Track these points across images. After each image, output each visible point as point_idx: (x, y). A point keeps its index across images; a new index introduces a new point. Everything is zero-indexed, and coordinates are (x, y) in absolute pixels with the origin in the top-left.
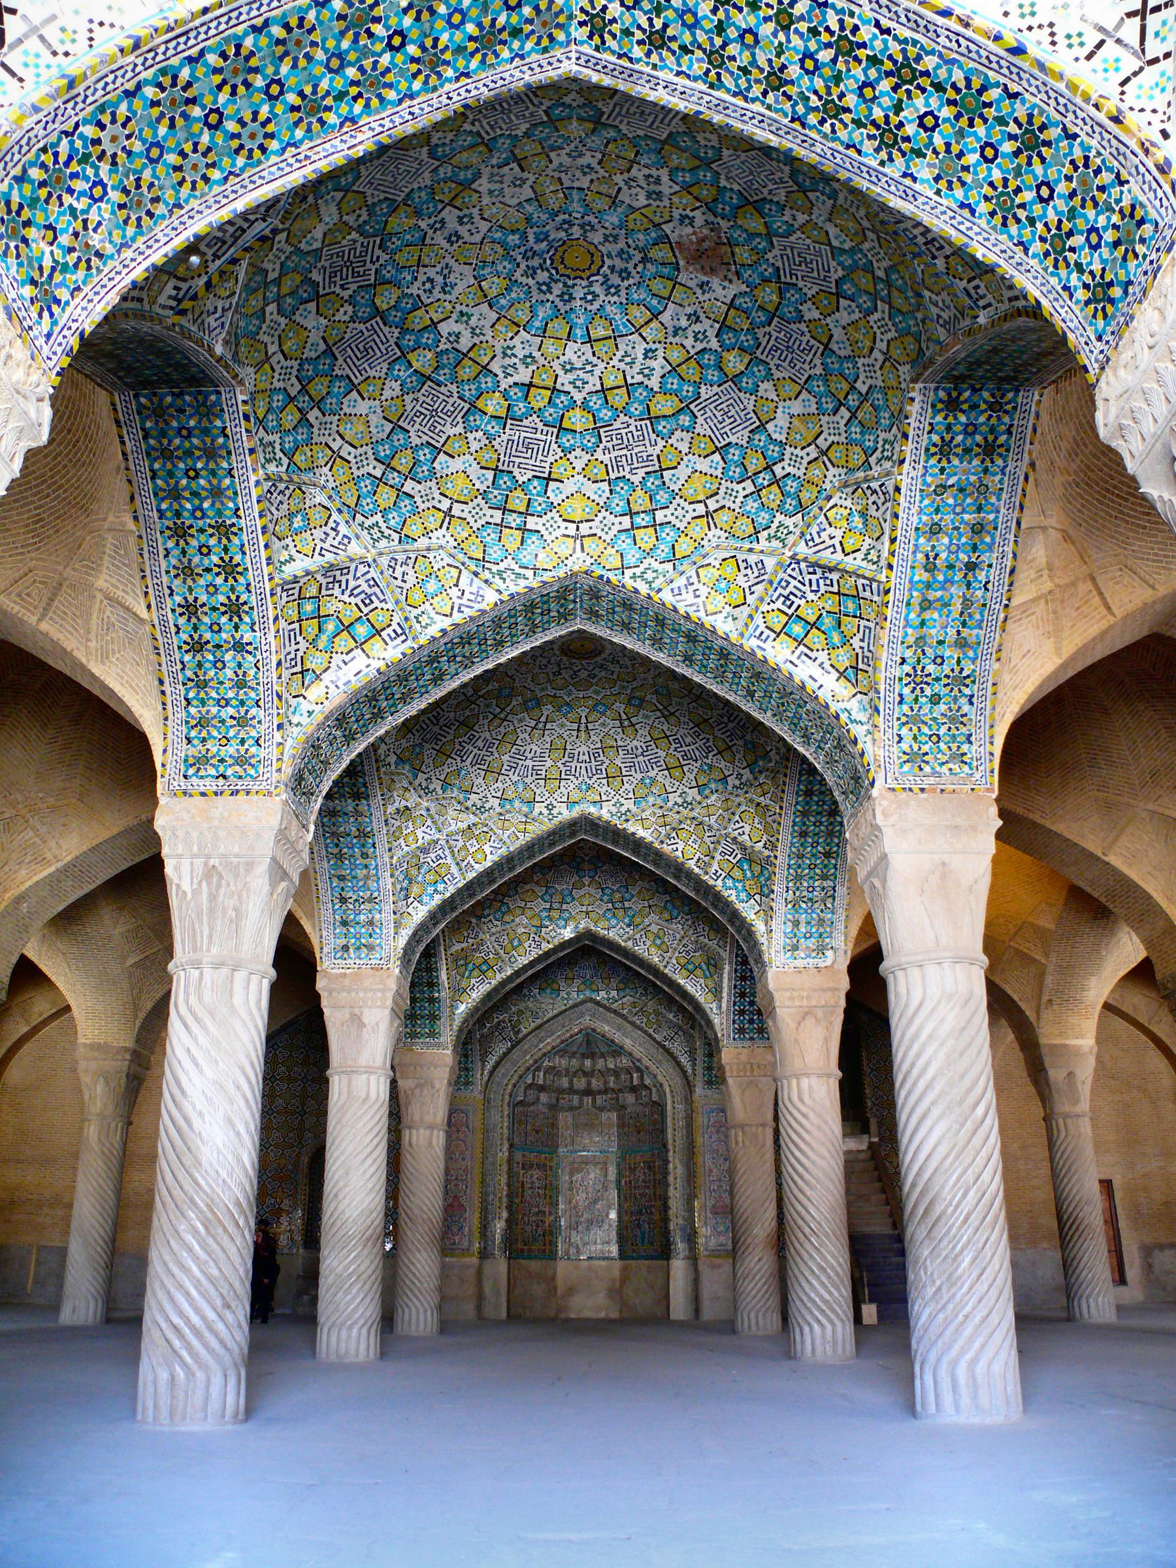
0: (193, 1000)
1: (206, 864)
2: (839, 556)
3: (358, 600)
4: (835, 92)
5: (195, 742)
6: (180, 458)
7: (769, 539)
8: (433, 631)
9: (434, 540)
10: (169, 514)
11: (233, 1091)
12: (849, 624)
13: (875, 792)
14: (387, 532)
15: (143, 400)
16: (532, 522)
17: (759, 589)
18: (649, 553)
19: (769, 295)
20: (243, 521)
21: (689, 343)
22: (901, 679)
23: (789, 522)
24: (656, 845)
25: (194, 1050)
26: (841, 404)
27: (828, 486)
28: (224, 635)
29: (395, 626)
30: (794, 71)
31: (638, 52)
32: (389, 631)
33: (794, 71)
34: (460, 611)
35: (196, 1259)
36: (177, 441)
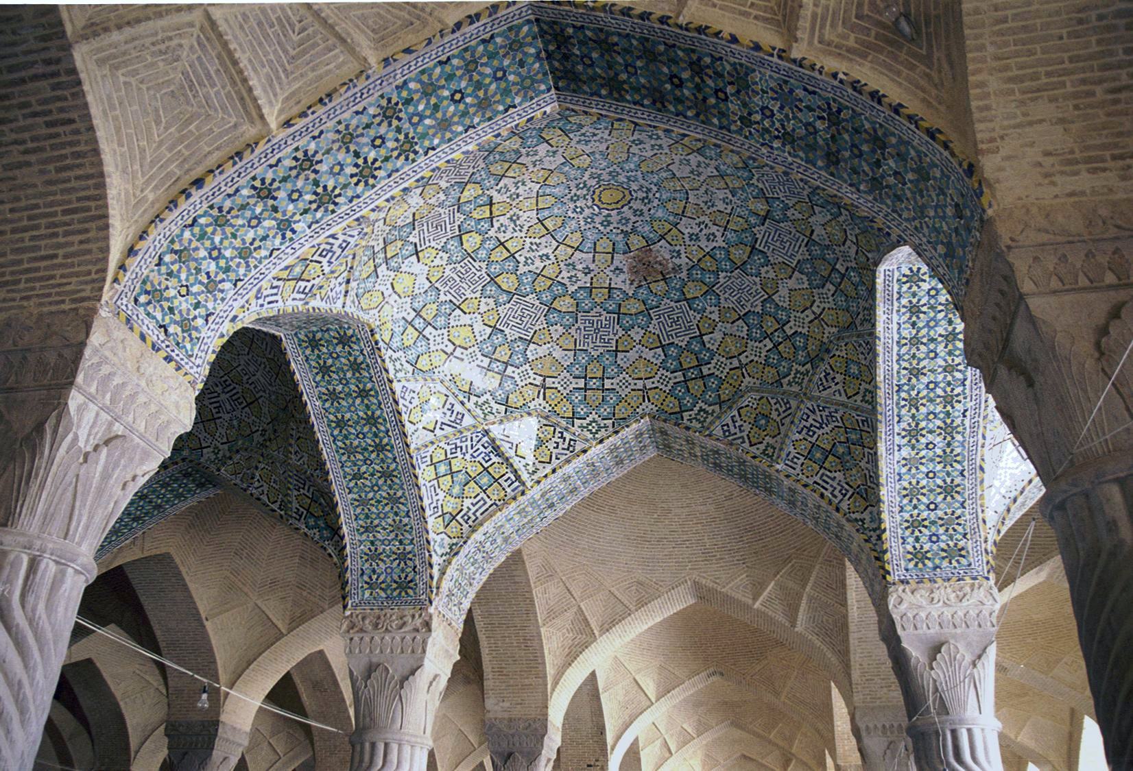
4: (924, 401)
5: (163, 269)
6: (471, 79)
10: (404, 94)
12: (473, 489)
15: (525, 29)
19: (634, 307)
20: (423, 158)
21: (565, 274)
26: (585, 378)
27: (532, 405)
28: (291, 207)
29: (309, 285)
30: (925, 380)
31: (904, 301)
33: (925, 380)
36: (488, 71)
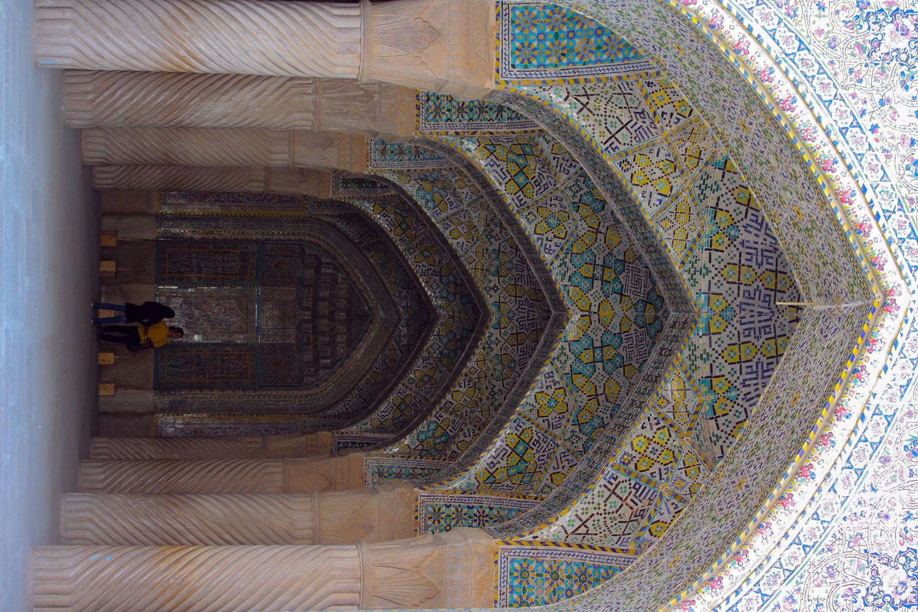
0: (295, 90)
1: (375, 92)
2: (551, 471)
3: (537, 178)
7: (573, 431)
8: (523, 222)
9: (580, 223)
11: (243, 116)
12: (517, 479)
13: (416, 489)
14: (578, 195)
16: (597, 283)
17: (545, 425)
18: (578, 358)
22: (481, 507)
23: (580, 444)
24: (464, 371)
25: (265, 93)
32: (522, 196)
34: (538, 239)
35: (151, 102)
